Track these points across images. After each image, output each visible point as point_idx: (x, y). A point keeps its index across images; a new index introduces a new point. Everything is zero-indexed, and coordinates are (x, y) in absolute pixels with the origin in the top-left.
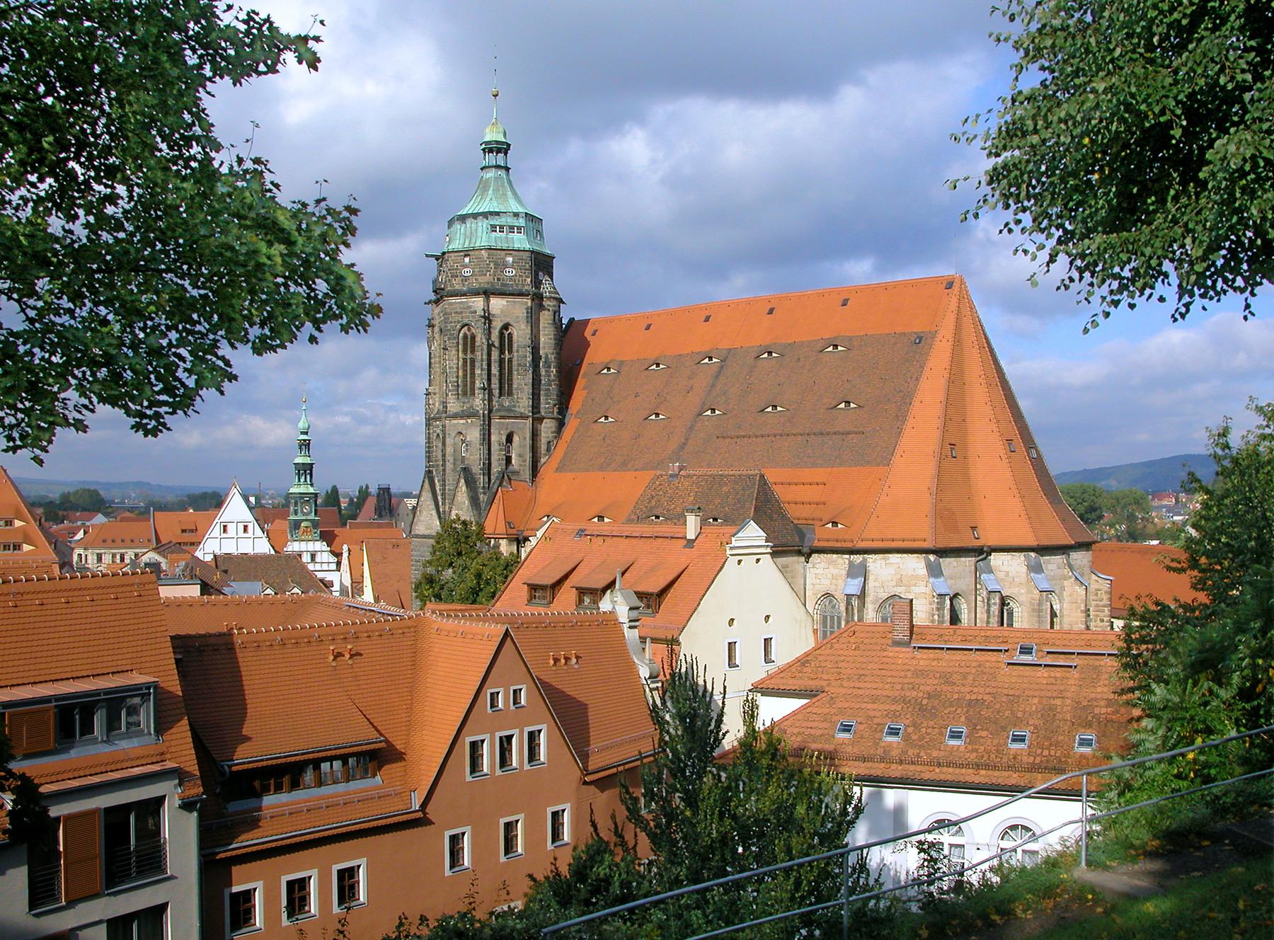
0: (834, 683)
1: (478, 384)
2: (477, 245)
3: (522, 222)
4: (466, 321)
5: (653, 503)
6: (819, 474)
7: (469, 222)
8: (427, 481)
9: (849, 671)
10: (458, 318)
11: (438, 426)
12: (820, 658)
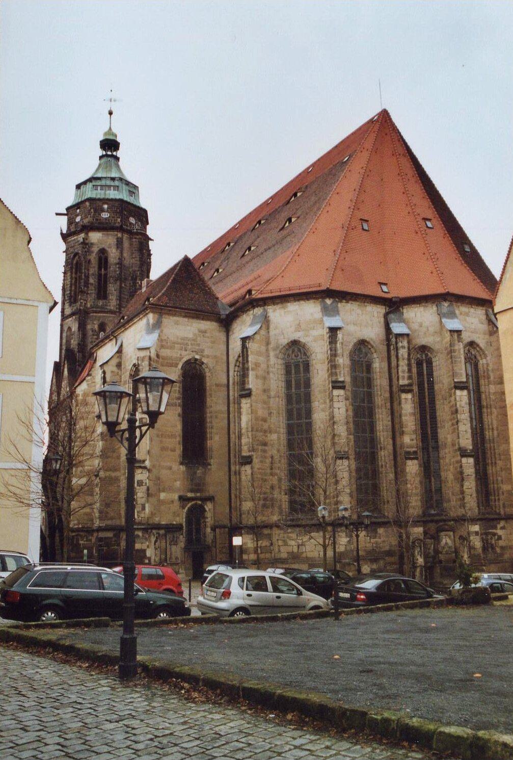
4: (76, 251)
7: (82, 187)
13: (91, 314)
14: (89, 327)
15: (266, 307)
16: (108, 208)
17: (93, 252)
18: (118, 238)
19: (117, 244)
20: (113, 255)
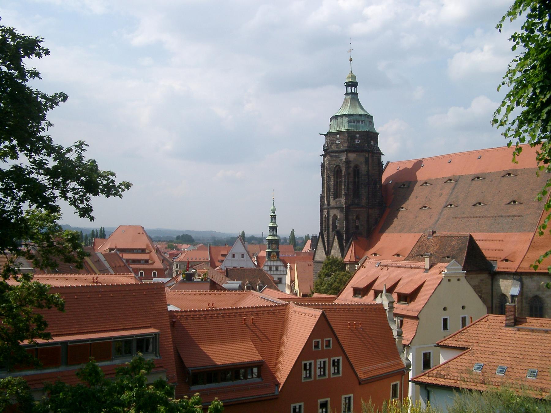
0: (475, 344)
1: (343, 193)
2: (343, 129)
3: (363, 118)
4: (338, 164)
5: (420, 248)
6: (500, 236)
7: (339, 118)
8: (320, 237)
9: (483, 339)
10: (334, 162)
11: (325, 212)
12: (470, 332)
13: (352, 209)
14: (350, 217)
15: (522, 276)
16: (359, 137)
17: (350, 167)
18: (366, 158)
19: (366, 162)
20: (363, 169)
